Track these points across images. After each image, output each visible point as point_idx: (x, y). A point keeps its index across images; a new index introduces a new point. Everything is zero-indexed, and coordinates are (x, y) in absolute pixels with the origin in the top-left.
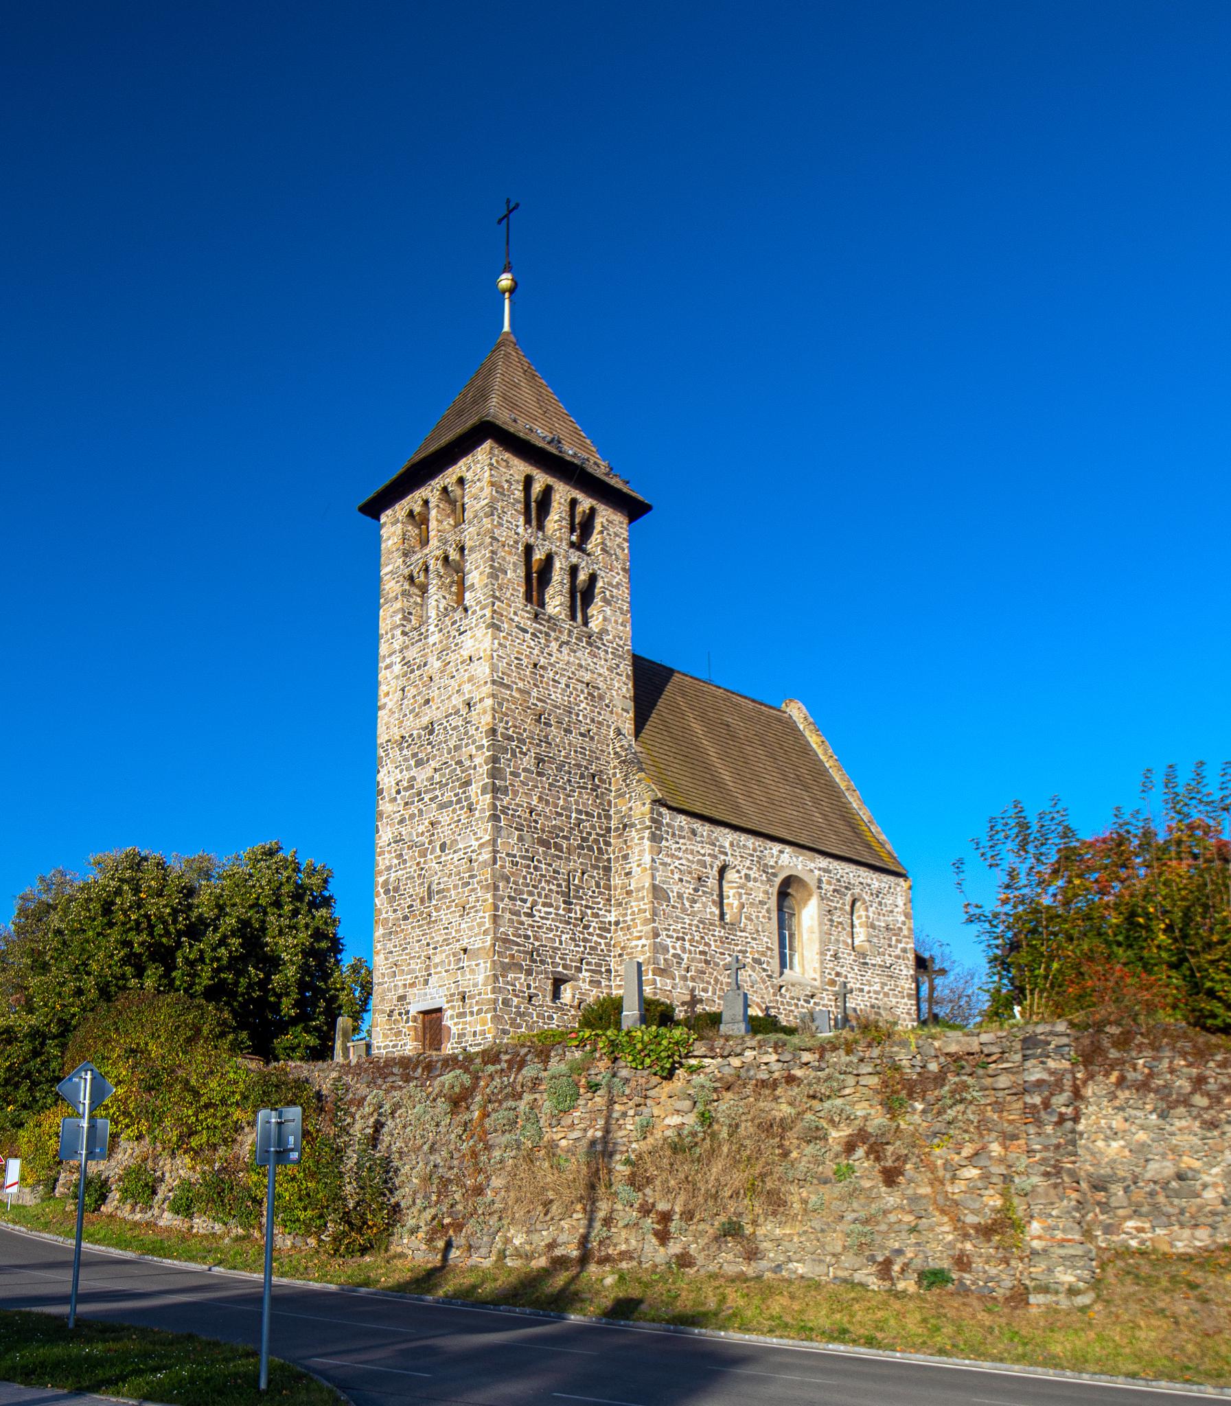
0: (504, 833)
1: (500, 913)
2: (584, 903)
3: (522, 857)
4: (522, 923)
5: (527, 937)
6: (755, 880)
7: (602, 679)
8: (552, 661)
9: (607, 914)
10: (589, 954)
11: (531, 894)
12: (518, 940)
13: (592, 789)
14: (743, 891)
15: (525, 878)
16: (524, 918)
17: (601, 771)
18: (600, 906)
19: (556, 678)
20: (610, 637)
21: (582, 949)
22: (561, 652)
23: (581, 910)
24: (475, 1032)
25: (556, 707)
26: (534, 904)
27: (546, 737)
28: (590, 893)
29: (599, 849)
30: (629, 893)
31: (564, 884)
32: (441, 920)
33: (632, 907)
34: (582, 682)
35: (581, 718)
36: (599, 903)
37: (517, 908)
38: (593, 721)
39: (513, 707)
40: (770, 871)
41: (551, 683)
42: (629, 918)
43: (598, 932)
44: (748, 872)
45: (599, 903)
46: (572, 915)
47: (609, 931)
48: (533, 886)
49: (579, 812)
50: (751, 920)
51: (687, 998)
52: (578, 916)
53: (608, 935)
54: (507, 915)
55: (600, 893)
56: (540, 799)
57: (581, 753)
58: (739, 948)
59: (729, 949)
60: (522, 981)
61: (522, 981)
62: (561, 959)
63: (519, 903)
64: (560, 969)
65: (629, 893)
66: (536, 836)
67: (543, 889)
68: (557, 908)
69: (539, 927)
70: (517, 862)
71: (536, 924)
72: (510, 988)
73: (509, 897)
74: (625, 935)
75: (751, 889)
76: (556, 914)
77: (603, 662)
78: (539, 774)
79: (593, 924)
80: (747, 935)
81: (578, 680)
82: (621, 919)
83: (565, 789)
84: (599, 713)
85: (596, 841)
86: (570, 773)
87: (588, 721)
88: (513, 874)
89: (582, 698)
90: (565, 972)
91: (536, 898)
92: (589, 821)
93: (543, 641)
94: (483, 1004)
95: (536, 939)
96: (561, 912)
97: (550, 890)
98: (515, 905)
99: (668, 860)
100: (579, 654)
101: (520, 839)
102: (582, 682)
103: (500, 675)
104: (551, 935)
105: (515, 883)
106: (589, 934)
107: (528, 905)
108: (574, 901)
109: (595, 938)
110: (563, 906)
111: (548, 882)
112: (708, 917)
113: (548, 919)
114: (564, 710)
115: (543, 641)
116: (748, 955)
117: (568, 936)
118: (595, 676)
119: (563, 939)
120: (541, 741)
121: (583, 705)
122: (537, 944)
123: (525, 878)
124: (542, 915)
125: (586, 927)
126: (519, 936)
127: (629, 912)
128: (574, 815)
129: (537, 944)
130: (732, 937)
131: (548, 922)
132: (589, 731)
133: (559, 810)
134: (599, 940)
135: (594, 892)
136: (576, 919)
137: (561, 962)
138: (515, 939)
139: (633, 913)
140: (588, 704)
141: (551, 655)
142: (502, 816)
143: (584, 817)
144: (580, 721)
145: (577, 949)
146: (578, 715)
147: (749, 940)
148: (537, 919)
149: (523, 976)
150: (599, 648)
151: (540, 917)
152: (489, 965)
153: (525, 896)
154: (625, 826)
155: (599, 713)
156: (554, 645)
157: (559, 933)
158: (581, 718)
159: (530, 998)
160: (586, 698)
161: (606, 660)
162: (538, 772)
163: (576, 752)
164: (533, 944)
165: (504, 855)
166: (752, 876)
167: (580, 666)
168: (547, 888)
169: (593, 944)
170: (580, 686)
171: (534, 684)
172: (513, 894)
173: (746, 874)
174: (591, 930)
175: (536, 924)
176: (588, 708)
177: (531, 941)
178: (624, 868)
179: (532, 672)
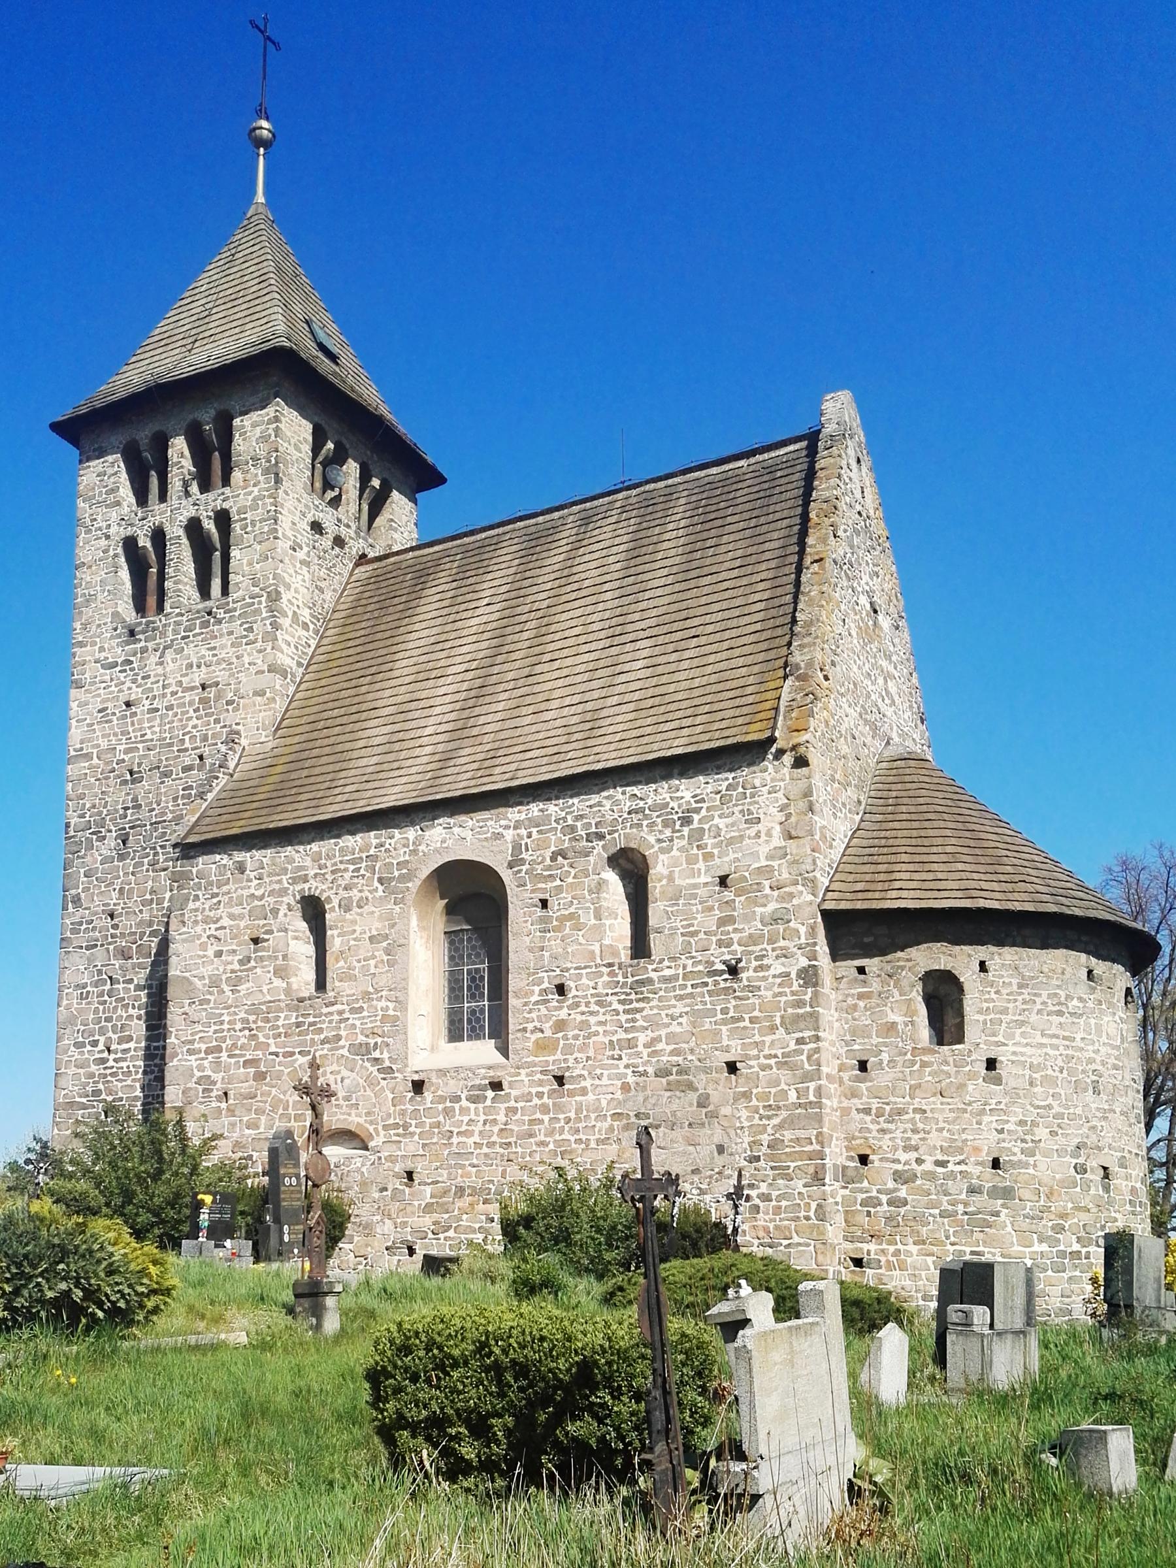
1: (63, 1070)
4: (92, 1075)
5: (96, 1093)
7: (224, 666)
11: (102, 1031)
12: (84, 1100)
14: (335, 932)
16: (93, 1068)
19: (154, 706)
37: (87, 1056)
38: (205, 738)
39: (93, 780)
40: (396, 874)
44: (345, 894)
50: (353, 978)
54: (72, 1070)
59: (303, 1043)
63: (89, 1048)
69: (113, 1075)
70: (88, 992)
75: (354, 922)
78: (122, 857)
91: (110, 1034)
102: (193, 688)
103: (78, 746)
104: (129, 1082)
107: (101, 1046)
111: (126, 1006)
112: (269, 998)
113: (124, 1060)
116: (342, 1043)
123: (96, 1011)
130: (311, 1019)
131: (124, 1064)
133: (148, 897)
144: (186, 750)
147: (346, 1015)
158: (187, 745)
163: (175, 799)
172: (81, 1039)
175: (108, 1071)
177: (103, 1096)
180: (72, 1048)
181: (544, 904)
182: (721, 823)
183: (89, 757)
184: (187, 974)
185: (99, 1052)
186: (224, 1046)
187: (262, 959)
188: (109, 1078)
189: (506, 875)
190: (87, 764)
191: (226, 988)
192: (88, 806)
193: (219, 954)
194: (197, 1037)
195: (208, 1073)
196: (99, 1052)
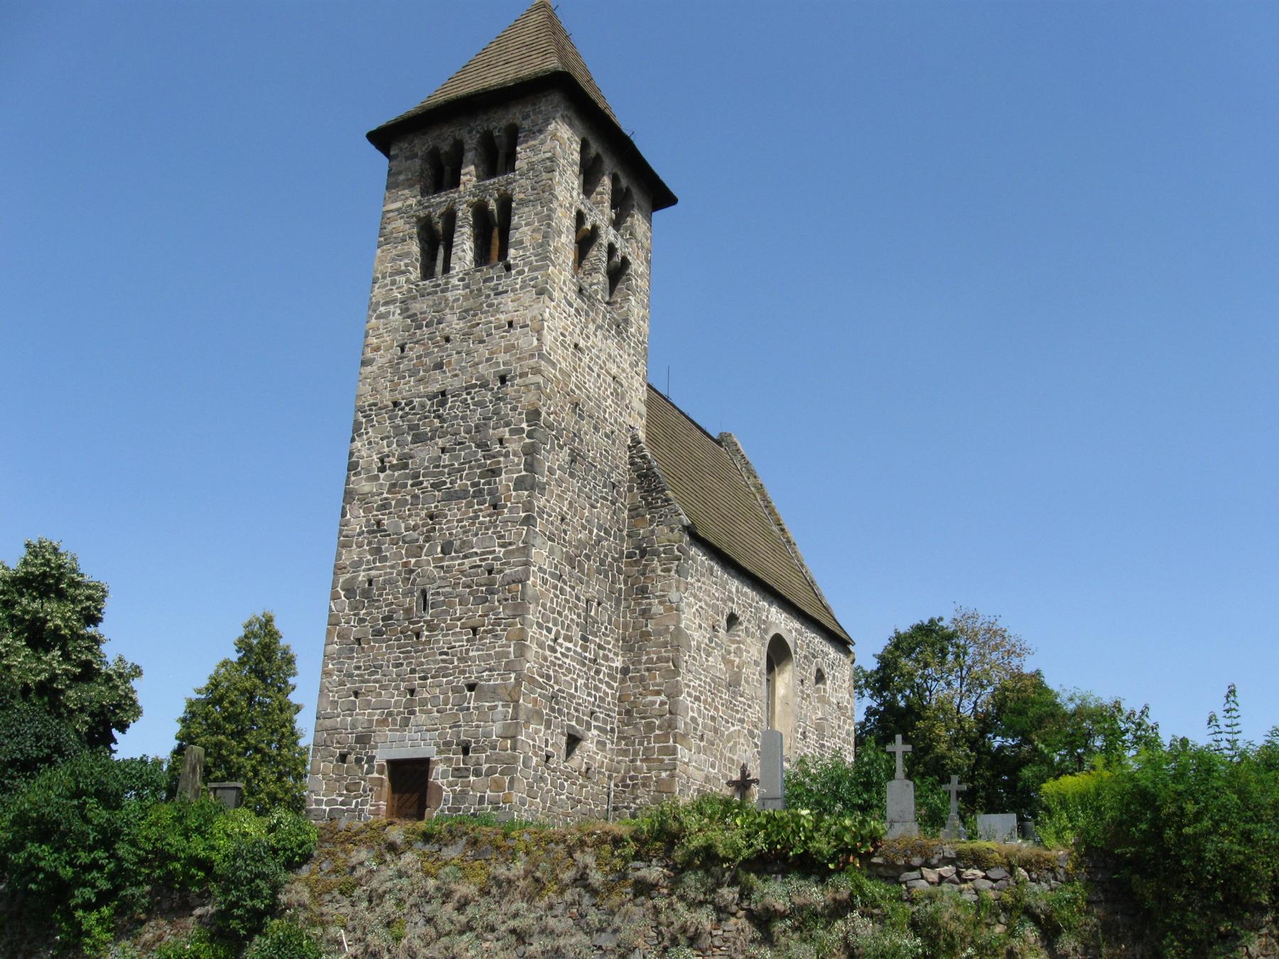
0: (538, 541)
1: (528, 643)
2: (597, 640)
3: (552, 575)
4: (545, 659)
5: (548, 677)
6: (753, 636)
7: (625, 375)
8: (589, 345)
9: (615, 657)
10: (599, 707)
12: (541, 680)
13: (611, 501)
15: (552, 602)
16: (548, 653)
17: (619, 482)
18: (610, 647)
19: (591, 365)
20: (633, 330)
21: (593, 700)
22: (596, 336)
23: (594, 649)
24: (482, 798)
25: (588, 397)
26: (558, 633)
27: (579, 430)
28: (603, 630)
29: (613, 575)
30: (646, 635)
31: (583, 614)
32: (438, 641)
33: (648, 653)
34: (610, 374)
35: (607, 416)
36: (609, 643)
37: (543, 639)
38: (616, 421)
41: (587, 369)
42: (643, 667)
43: (607, 679)
45: (609, 643)
46: (587, 655)
47: (614, 679)
48: (560, 614)
49: (600, 528)
51: (736, 776)
52: (592, 657)
53: (615, 685)
54: (534, 646)
55: (612, 631)
56: (570, 503)
57: (605, 457)
58: (738, 716)
60: (541, 735)
61: (541, 735)
62: (577, 710)
63: (544, 632)
64: (573, 723)
65: (646, 635)
66: (564, 550)
67: (566, 617)
68: (575, 645)
69: (560, 666)
71: (558, 662)
72: (531, 743)
73: (538, 623)
74: (636, 687)
76: (575, 652)
77: (626, 357)
78: (572, 475)
79: (604, 668)
80: (745, 701)
81: (607, 371)
82: (631, 667)
83: (590, 498)
84: (621, 414)
85: (611, 565)
86: (595, 478)
87: (613, 421)
88: (542, 593)
89: (609, 393)
90: (578, 727)
92: (606, 540)
93: (583, 320)
94: (496, 761)
95: (556, 683)
96: (579, 649)
97: (572, 620)
98: (541, 633)
99: (692, 599)
100: (609, 341)
101: (551, 552)
102: (610, 374)
104: (568, 679)
105: (544, 606)
106: (601, 681)
107: (552, 636)
108: (590, 637)
109: (604, 687)
110: (581, 642)
112: (718, 674)
113: (567, 657)
114: (595, 403)
115: (583, 320)
117: (583, 681)
118: (620, 371)
119: (579, 684)
120: (575, 435)
121: (609, 401)
122: (556, 688)
124: (563, 651)
125: (598, 672)
126: (542, 677)
127: (644, 658)
128: (595, 531)
129: (556, 688)
131: (568, 661)
132: (612, 432)
133: (584, 521)
134: (607, 690)
135: (606, 628)
136: (590, 660)
137: (576, 714)
138: (538, 678)
139: (650, 661)
140: (613, 401)
141: (589, 338)
142: (538, 520)
143: (602, 534)
145: (589, 698)
146: (605, 412)
148: (559, 655)
149: (542, 728)
150: (625, 341)
151: (561, 652)
152: (510, 711)
153: (550, 625)
154: (643, 553)
155: (621, 414)
156: (592, 327)
157: (575, 677)
159: (548, 757)
160: (612, 394)
161: (629, 355)
162: (570, 472)
163: (601, 454)
164: (553, 688)
165: (536, 569)
166: (752, 630)
167: (610, 356)
168: (570, 617)
169: (602, 694)
170: (609, 379)
171: (574, 368)
172: (540, 620)
173: (746, 627)
174: (601, 676)
175: (558, 662)
176: (613, 405)
177: (552, 683)
178: (640, 604)
179: (572, 352)
180: (535, 625)
181: (802, 681)
182: (839, 675)
183: (554, 365)
184: (688, 632)
185: (552, 640)
186: (702, 698)
187: (716, 643)
188: (557, 668)
189: (793, 656)
190: (553, 371)
191: (704, 656)
192: (552, 409)
193: (700, 626)
194: (692, 684)
195: (696, 715)
196: (552, 640)
